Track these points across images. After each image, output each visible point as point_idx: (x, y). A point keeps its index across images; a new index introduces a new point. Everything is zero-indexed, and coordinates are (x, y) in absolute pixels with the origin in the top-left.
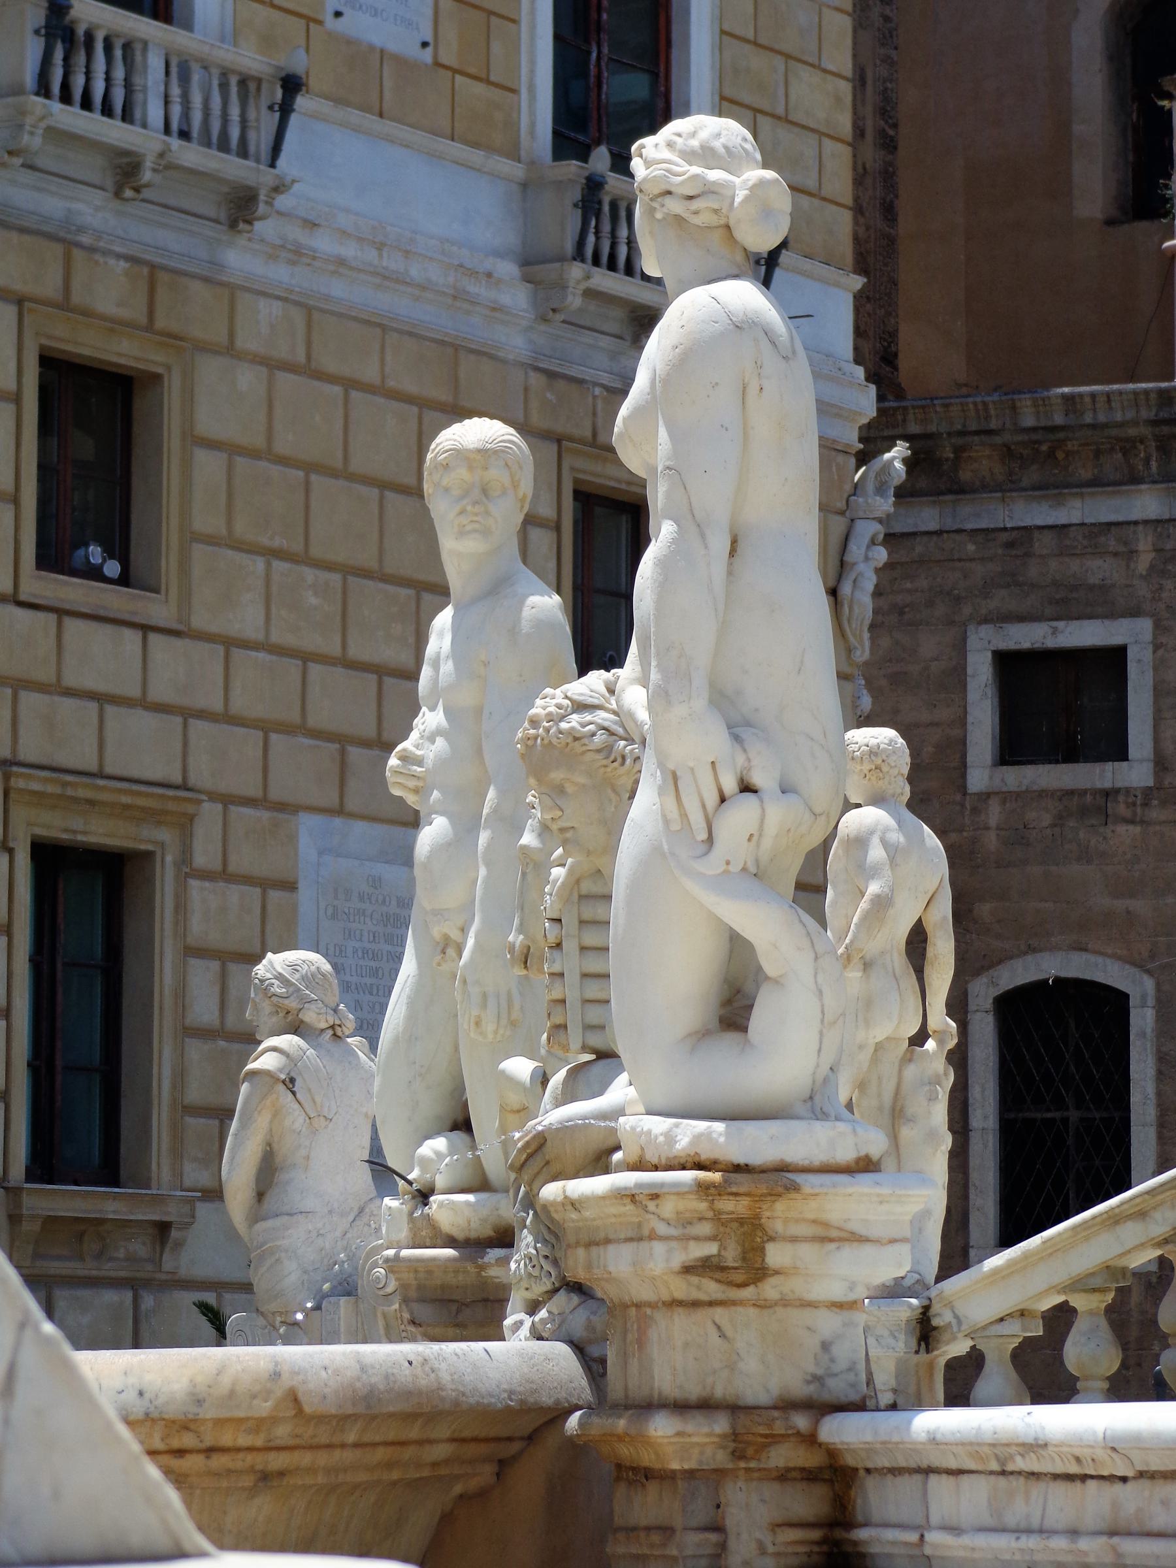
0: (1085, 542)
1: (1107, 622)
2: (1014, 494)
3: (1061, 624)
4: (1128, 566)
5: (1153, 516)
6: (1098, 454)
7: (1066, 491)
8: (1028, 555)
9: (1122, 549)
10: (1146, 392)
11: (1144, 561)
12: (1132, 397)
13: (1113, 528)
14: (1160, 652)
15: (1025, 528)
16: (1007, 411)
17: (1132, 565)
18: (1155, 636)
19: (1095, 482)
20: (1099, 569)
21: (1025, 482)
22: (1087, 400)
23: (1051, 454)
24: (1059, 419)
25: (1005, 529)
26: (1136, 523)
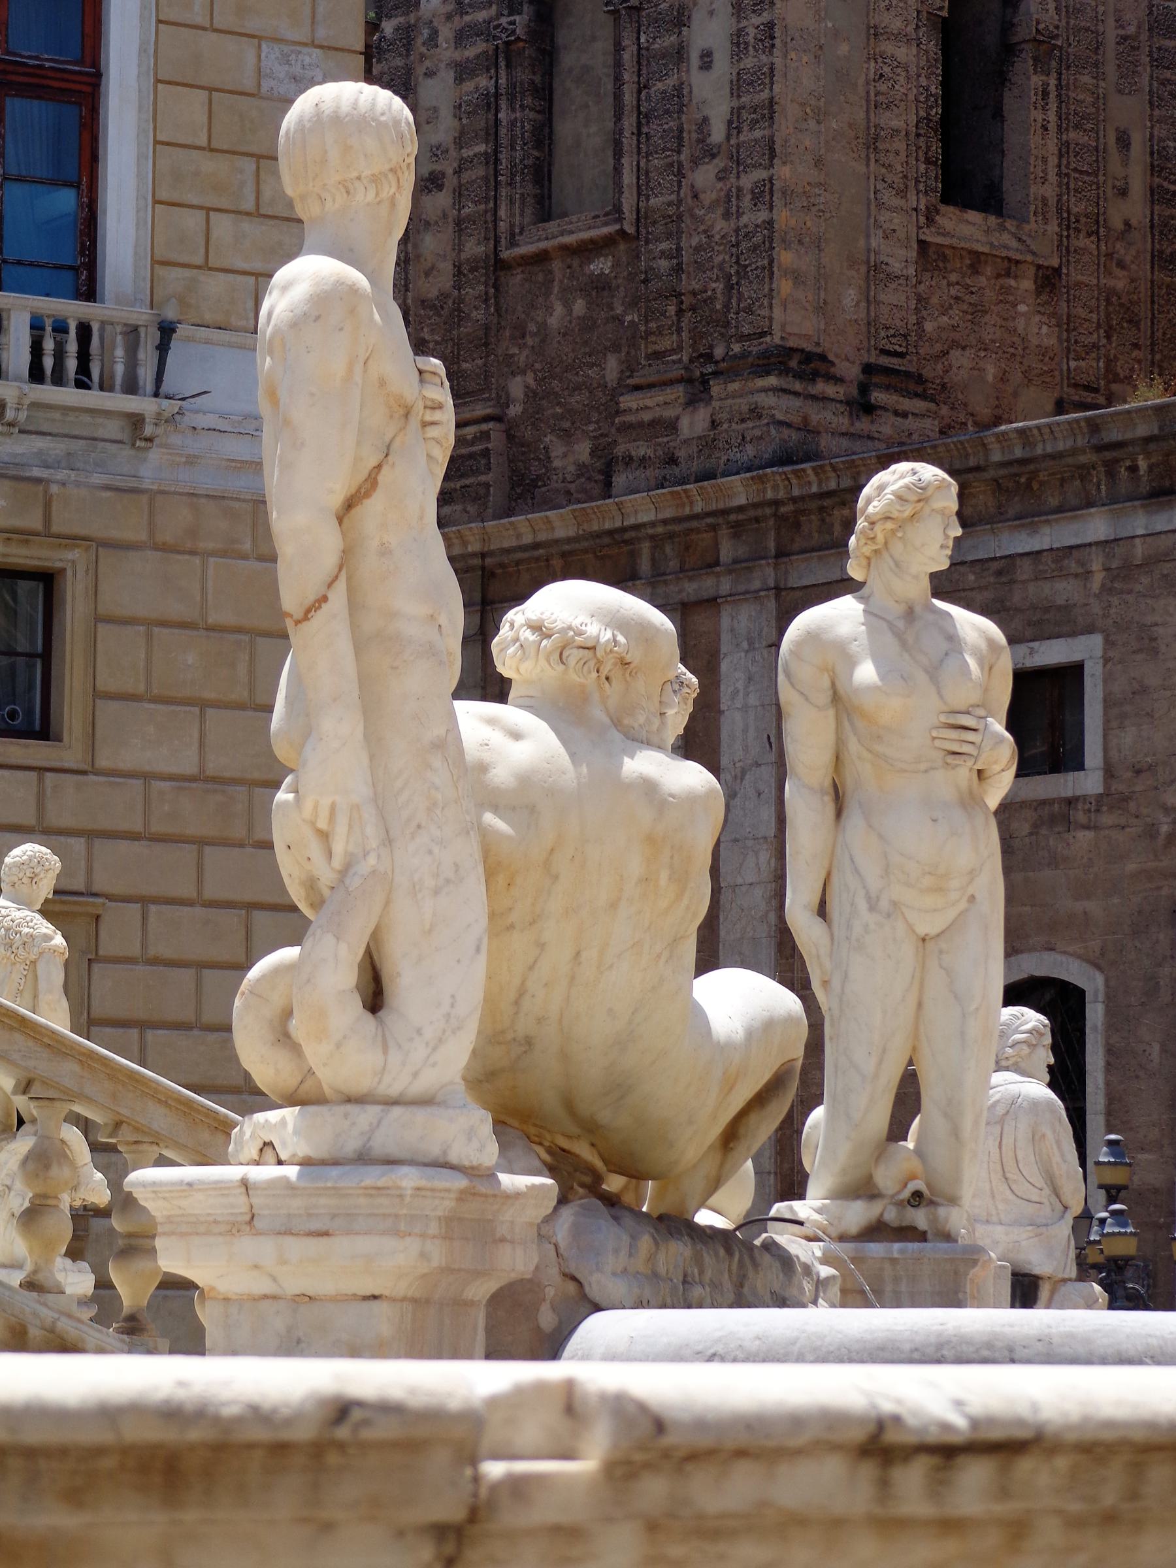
0: (1053, 566)
1: (1069, 640)
2: (1000, 525)
3: (1035, 645)
4: (1085, 586)
5: (1102, 538)
6: (1063, 481)
7: (1036, 519)
8: (1012, 582)
9: (1081, 570)
10: (1077, 421)
11: (1098, 579)
12: (1067, 427)
13: (1074, 551)
14: (1110, 664)
15: (1010, 556)
16: (979, 448)
17: (1088, 586)
18: (1105, 650)
19: (1060, 510)
20: (1064, 591)
21: (1011, 513)
22: (1035, 432)
23: (1028, 486)
24: (1018, 453)
25: (995, 559)
26: (1090, 545)
